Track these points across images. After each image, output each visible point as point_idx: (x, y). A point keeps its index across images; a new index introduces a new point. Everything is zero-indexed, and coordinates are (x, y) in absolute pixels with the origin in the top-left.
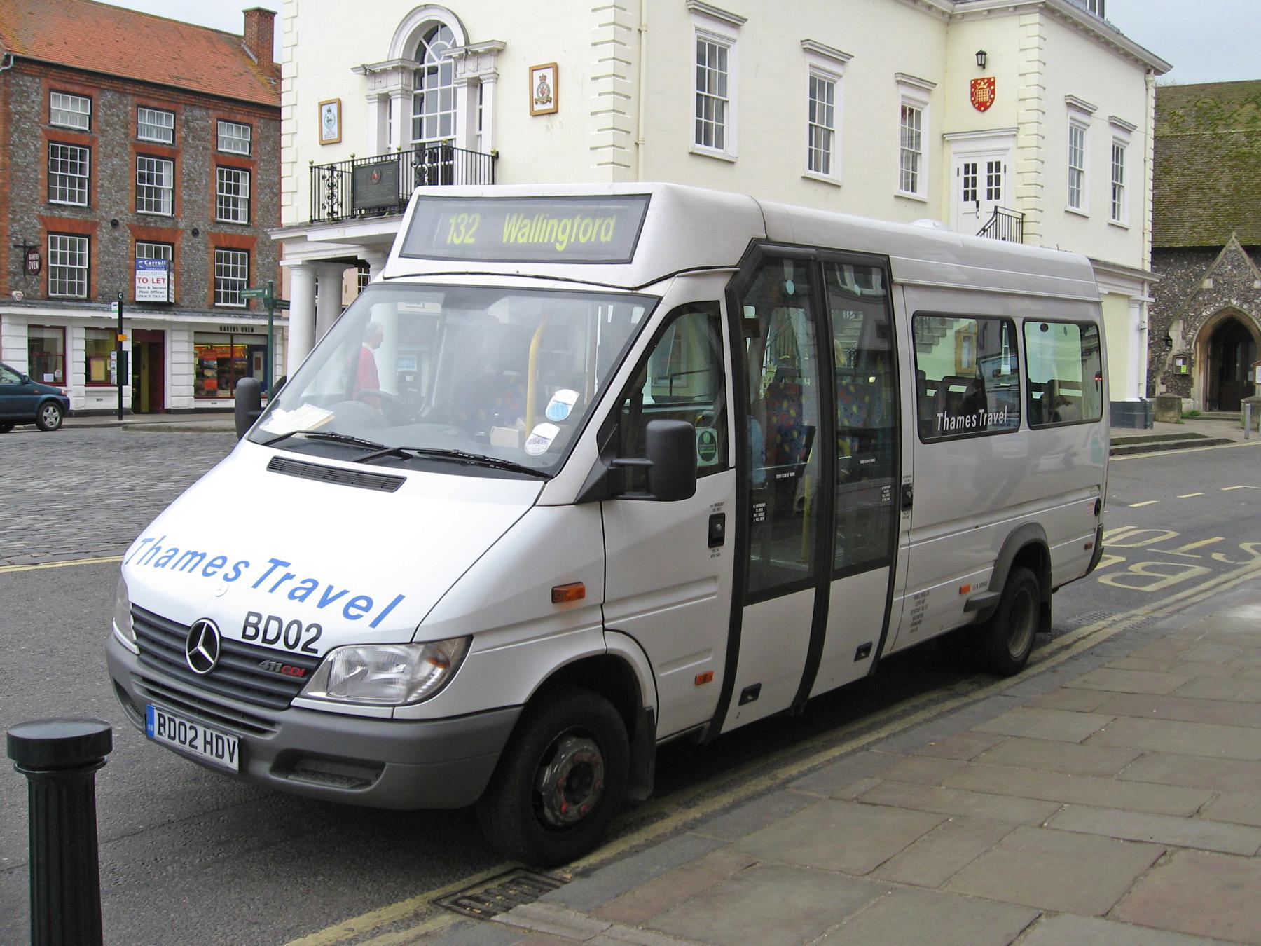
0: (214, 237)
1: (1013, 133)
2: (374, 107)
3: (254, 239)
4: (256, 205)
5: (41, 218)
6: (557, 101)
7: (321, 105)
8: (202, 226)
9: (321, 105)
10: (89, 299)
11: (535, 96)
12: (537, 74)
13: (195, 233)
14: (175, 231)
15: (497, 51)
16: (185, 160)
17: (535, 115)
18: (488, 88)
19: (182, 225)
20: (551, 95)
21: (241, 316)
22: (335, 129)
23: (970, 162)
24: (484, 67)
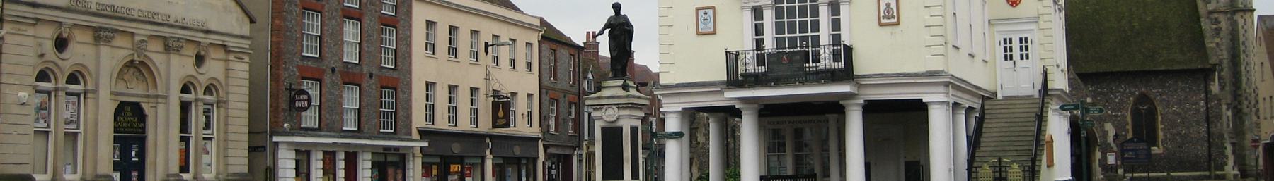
0: (380, 77)
1: (1036, 20)
2: (748, 16)
3: (397, 80)
4: (399, 54)
7: (697, 9)
8: (375, 72)
9: (697, 9)
10: (320, 129)
13: (371, 76)
14: (362, 75)
16: (366, 20)
17: (881, 25)
19: (365, 71)
21: (390, 139)
22: (711, 25)
23: (1008, 37)
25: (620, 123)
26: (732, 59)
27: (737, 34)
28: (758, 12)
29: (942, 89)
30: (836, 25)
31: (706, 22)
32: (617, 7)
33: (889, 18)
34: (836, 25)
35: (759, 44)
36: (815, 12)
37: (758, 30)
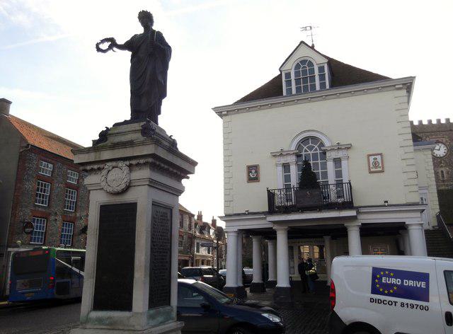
2: (280, 169)
5: (32, 211)
6: (383, 168)
11: (371, 166)
12: (372, 159)
15: (348, 147)
17: (371, 172)
18: (344, 163)
20: (380, 165)
24: (340, 154)
25: (129, 198)
26: (271, 196)
27: (273, 179)
28: (286, 167)
29: (418, 214)
30: (339, 174)
31: (253, 174)
32: (146, 18)
33: (376, 166)
34: (339, 174)
35: (288, 188)
36: (324, 166)
37: (287, 178)
